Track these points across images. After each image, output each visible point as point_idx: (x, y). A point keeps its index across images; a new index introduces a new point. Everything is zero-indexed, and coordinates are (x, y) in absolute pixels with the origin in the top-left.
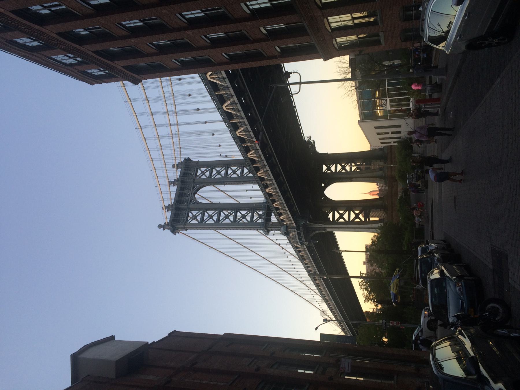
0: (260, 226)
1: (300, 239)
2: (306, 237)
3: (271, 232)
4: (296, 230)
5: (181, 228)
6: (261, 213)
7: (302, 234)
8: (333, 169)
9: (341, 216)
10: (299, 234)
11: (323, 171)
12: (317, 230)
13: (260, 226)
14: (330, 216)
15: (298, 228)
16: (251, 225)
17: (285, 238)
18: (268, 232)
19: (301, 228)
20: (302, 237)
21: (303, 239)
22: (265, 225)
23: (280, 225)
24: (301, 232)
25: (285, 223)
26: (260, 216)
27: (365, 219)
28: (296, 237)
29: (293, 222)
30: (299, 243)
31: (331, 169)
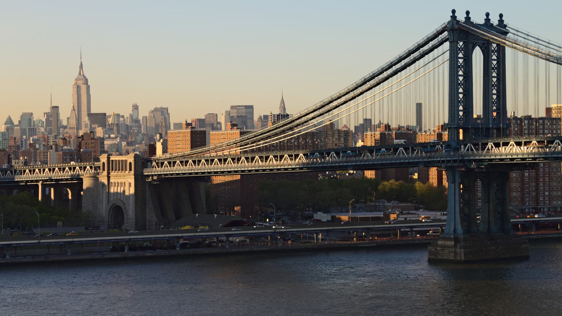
1: (449, 161)
4: (461, 158)
7: (455, 164)
10: (455, 161)
21: (449, 165)
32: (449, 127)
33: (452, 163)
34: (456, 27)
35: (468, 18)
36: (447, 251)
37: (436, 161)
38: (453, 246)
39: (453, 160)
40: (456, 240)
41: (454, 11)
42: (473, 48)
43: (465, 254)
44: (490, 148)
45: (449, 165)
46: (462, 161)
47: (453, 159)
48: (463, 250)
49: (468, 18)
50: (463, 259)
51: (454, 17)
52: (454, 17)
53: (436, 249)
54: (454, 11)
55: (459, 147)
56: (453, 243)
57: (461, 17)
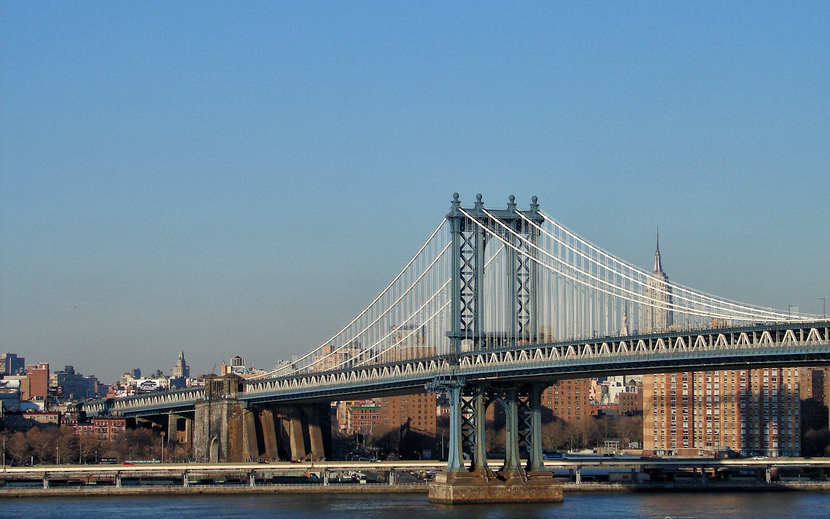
0: (456, 330)
1: (442, 378)
4: (452, 375)
6: (472, 327)
10: (448, 378)
16: (457, 316)
18: (450, 337)
21: (442, 382)
24: (450, 381)
33: (452, 380)
34: (456, 214)
38: (446, 482)
41: (457, 196)
43: (455, 492)
44: (479, 361)
45: (442, 382)
46: (454, 378)
47: (446, 375)
50: (452, 498)
51: (456, 202)
52: (456, 202)
53: (434, 487)
54: (457, 196)
56: (445, 478)
57: (467, 202)
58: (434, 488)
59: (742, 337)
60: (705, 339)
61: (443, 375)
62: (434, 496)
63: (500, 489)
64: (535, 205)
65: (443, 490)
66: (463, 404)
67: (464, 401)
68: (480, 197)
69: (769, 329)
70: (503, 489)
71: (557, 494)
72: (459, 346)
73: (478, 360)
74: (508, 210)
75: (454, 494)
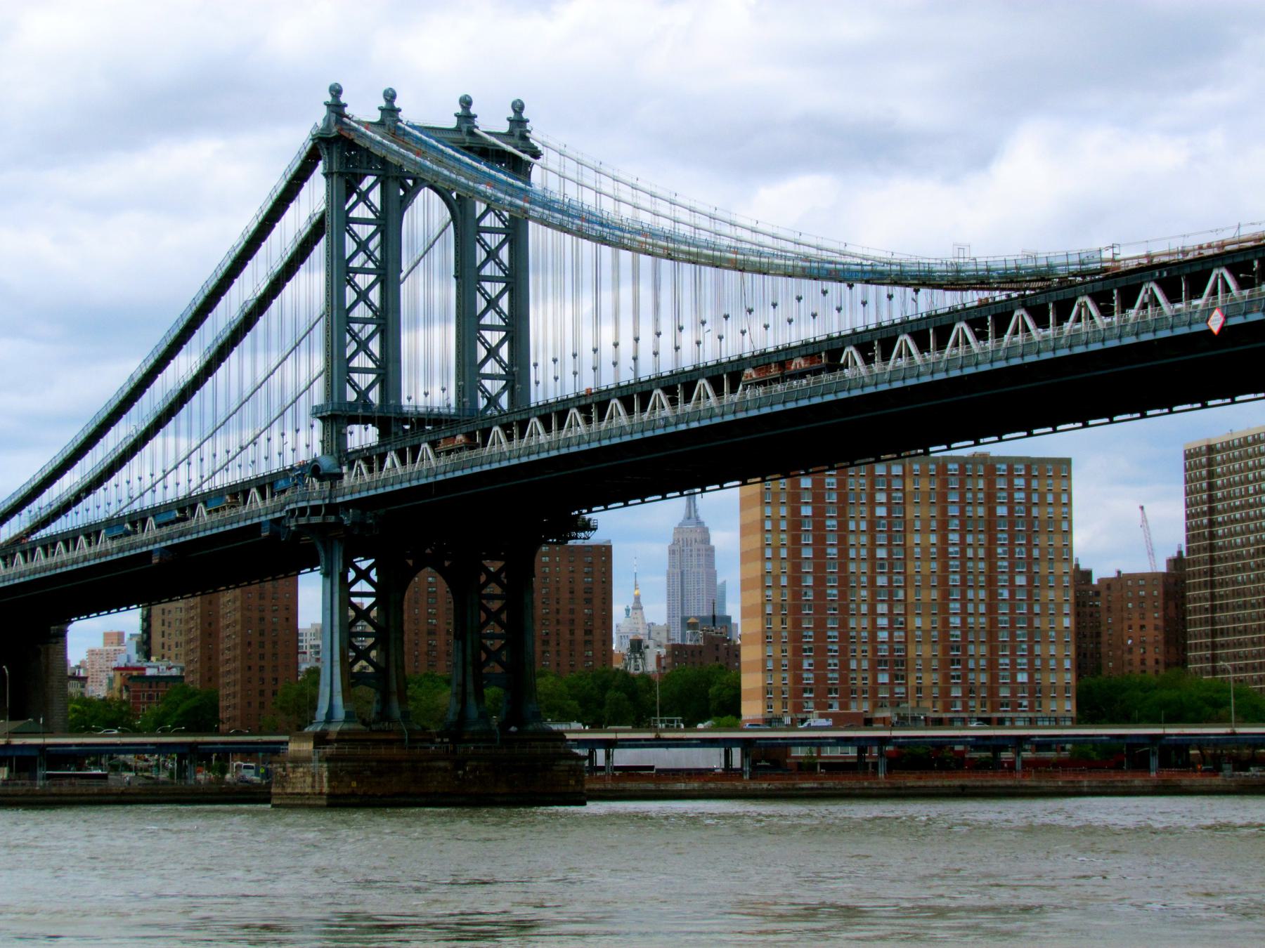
0: (336, 399)
2: (309, 527)
3: (318, 424)
5: (331, 167)
6: (374, 396)
7: (316, 520)
8: (494, 589)
9: (362, 614)
10: (316, 510)
11: (486, 563)
12: (326, 552)
13: (336, 399)
14: (363, 586)
15: (332, 508)
16: (338, 370)
17: (303, 456)
19: (332, 519)
20: (309, 520)
21: (303, 521)
22: (340, 415)
23: (339, 457)
25: (345, 469)
26: (363, 394)
27: (353, 675)
28: (308, 501)
29: (348, 498)
30: (292, 506)
31: (493, 585)
32: (319, 415)
35: (390, 111)
36: (301, 770)
37: (293, 511)
39: (313, 508)
40: (320, 740)
41: (336, 91)
42: (411, 193)
43: (333, 776)
47: (312, 503)
48: (325, 765)
49: (390, 111)
50: (326, 790)
51: (336, 108)
52: (336, 108)
54: (336, 91)
55: (337, 470)
58: (284, 770)
59: (1080, 306)
60: (975, 333)
61: (304, 504)
62: (283, 787)
63: (440, 769)
64: (518, 121)
65: (304, 773)
66: (352, 575)
67: (357, 569)
68: (390, 96)
69: (1161, 274)
70: (445, 770)
71: (572, 782)
72: (342, 438)
73: (388, 463)
74: (458, 130)
75: (330, 781)
